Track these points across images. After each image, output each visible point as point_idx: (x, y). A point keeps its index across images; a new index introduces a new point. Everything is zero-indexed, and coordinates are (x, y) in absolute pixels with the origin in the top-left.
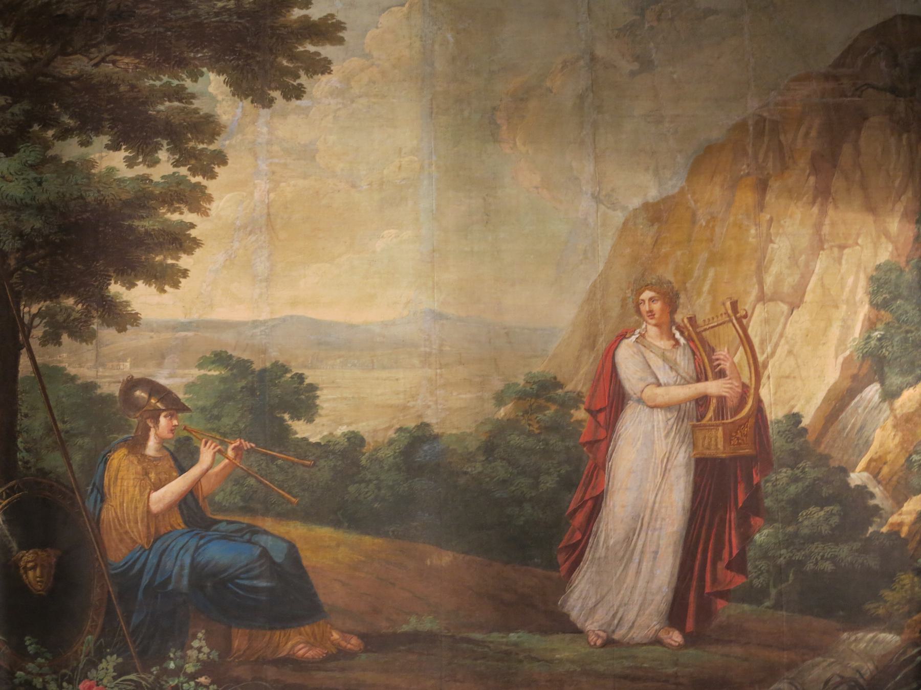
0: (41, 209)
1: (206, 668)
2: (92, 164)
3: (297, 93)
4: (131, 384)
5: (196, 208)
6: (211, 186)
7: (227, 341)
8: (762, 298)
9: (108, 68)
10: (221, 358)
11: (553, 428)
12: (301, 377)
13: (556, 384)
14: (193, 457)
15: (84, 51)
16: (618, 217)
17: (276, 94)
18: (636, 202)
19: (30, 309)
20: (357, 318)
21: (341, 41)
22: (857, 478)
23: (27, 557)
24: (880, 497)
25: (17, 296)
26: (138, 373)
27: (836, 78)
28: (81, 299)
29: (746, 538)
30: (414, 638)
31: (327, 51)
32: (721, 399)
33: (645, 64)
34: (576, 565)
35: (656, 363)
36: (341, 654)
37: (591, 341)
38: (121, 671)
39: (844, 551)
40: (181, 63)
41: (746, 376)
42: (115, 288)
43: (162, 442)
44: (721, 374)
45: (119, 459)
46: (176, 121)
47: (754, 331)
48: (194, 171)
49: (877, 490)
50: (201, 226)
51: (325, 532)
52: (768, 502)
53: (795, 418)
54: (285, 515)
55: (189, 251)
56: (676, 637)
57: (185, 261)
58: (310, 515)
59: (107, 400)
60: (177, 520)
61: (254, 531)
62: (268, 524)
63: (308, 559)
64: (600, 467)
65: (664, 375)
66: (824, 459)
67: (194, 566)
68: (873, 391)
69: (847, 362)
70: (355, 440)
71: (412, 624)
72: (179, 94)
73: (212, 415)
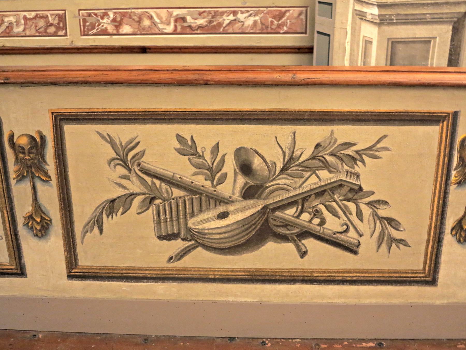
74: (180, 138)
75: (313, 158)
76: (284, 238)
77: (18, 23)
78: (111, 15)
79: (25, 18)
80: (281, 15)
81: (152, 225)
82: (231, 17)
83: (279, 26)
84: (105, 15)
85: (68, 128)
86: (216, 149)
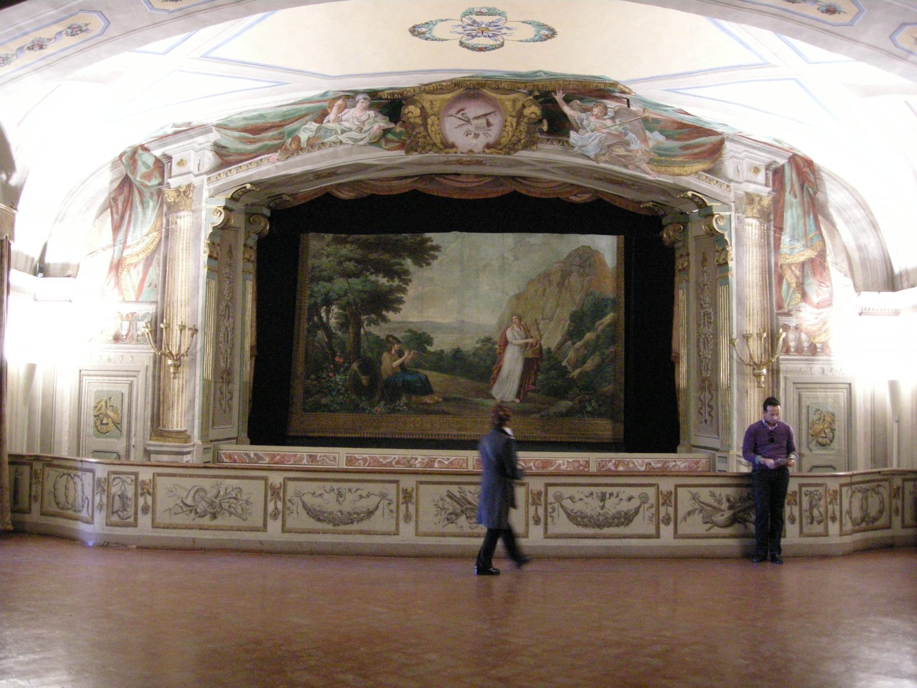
0: (366, 292)
1: (406, 404)
2: (379, 281)
3: (428, 264)
4: (388, 336)
5: (404, 293)
6: (408, 288)
7: (412, 326)
8: (543, 319)
9: (382, 257)
10: (410, 331)
11: (490, 350)
12: (429, 336)
13: (491, 339)
14: (403, 354)
15: (376, 252)
16: (508, 298)
17: (424, 265)
18: (513, 294)
19: (364, 317)
20: (444, 321)
21: (440, 251)
22: (564, 364)
23: (363, 377)
24: (570, 368)
25: (360, 314)
26: (390, 334)
27: (565, 262)
28: (376, 315)
29: (536, 378)
30: (455, 399)
31: (437, 253)
32: (532, 344)
33: (517, 258)
34: (495, 382)
35: (516, 334)
36: (438, 402)
37: (500, 328)
38: (385, 405)
39: (560, 382)
40: (401, 256)
41: (538, 338)
42: (384, 313)
43: (396, 350)
44: (532, 337)
45: (385, 355)
46: (399, 270)
47: (541, 327)
48: (404, 284)
49: (568, 367)
50: (405, 298)
51: (434, 373)
52: (542, 369)
53: (549, 349)
54: (424, 369)
55: (402, 304)
56: (518, 401)
57: (401, 306)
58: (430, 369)
59: (382, 340)
60: (400, 371)
61: (418, 373)
62: (421, 371)
63: (430, 379)
64: (501, 360)
65: (518, 337)
66: (556, 359)
67: (404, 381)
68: (569, 343)
69: (563, 336)
70: (442, 351)
71: (455, 395)
72: (400, 264)
73: (407, 344)
74: (710, 492)
75: (747, 497)
76: (740, 522)
77: (564, 464)
78: (613, 461)
79: (568, 462)
80: (697, 463)
81: (701, 519)
82: (674, 463)
83: (698, 468)
84: (611, 461)
85: (679, 489)
86: (720, 495)
